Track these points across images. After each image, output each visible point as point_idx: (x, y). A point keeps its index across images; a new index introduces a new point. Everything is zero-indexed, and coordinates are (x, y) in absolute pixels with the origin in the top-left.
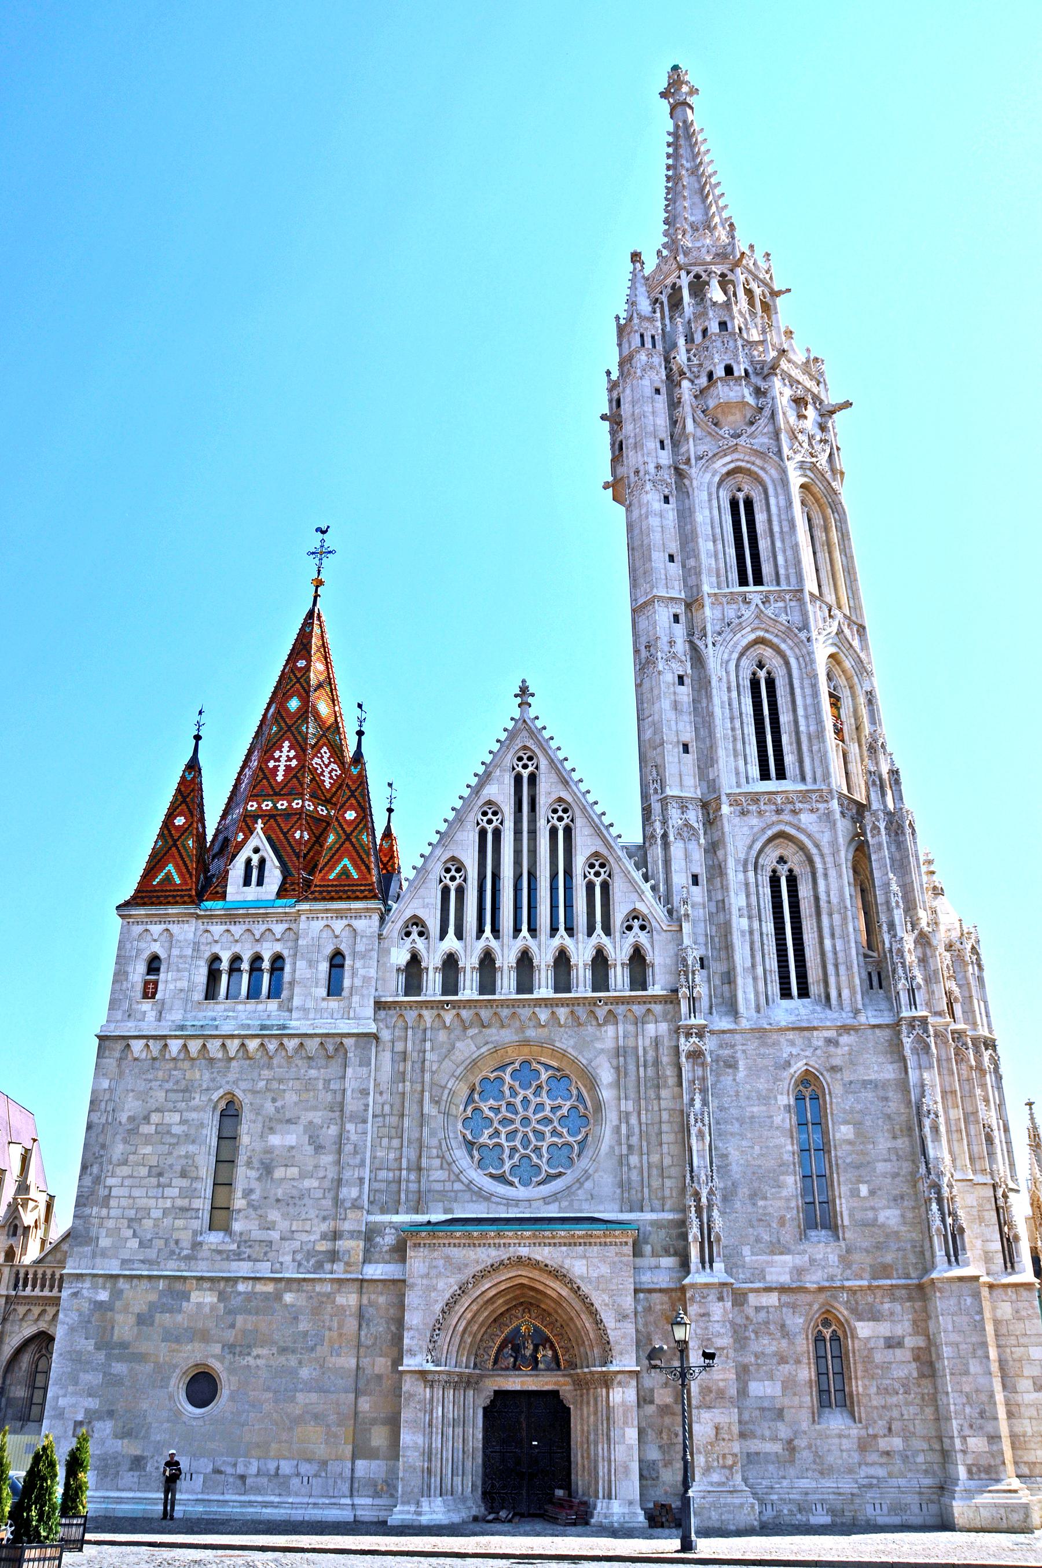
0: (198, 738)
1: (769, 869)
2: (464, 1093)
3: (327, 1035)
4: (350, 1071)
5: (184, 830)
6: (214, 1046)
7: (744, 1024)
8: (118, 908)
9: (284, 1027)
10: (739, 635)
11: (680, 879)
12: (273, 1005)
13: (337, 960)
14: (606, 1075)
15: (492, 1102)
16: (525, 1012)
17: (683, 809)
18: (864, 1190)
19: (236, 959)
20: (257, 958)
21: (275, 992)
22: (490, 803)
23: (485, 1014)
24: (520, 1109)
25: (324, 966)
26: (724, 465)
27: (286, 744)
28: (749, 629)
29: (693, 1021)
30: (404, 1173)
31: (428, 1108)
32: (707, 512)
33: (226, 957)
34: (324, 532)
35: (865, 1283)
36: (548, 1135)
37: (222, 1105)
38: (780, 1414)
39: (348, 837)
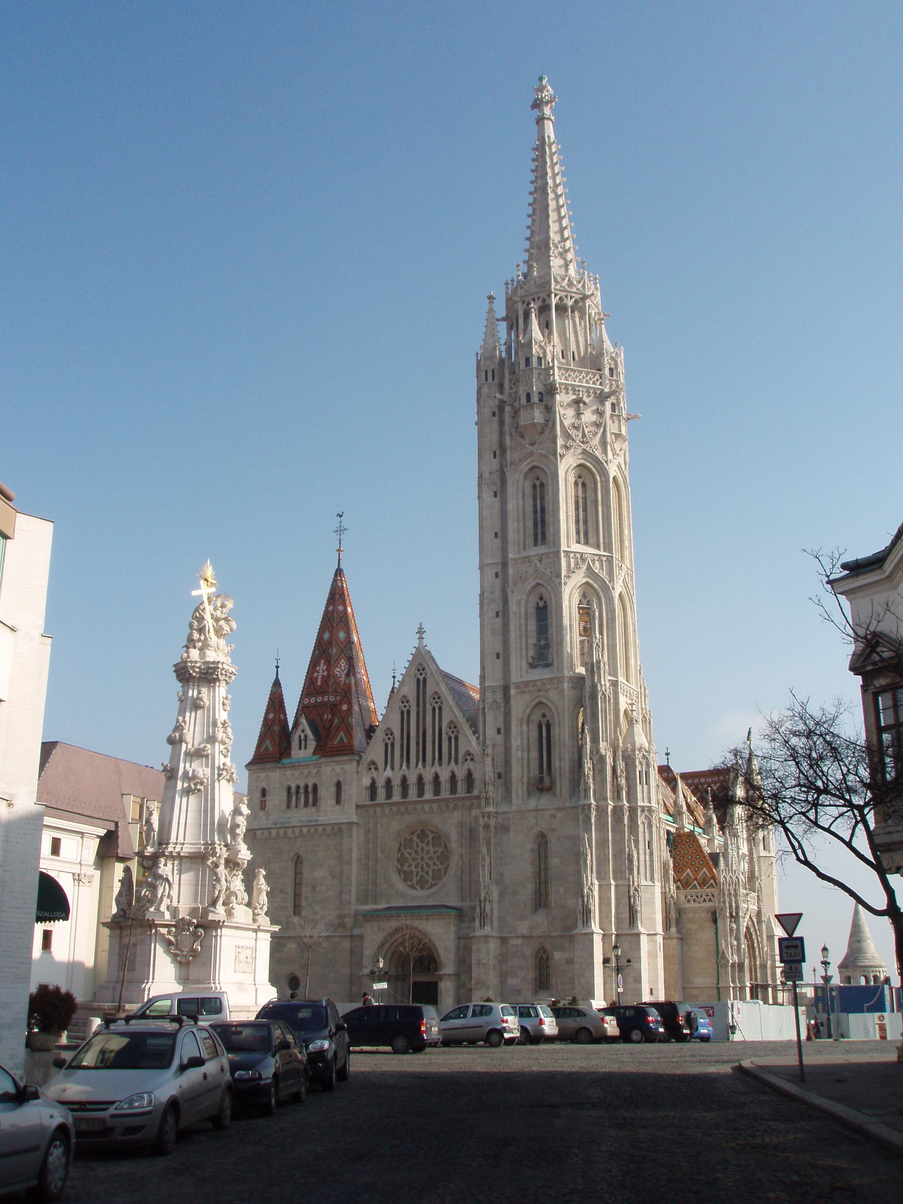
0: (277, 667)
1: (537, 722)
2: (396, 846)
3: (335, 824)
4: (344, 841)
5: (273, 721)
6: (289, 831)
7: (514, 808)
8: (246, 766)
9: (316, 821)
10: (526, 583)
11: (491, 732)
12: (314, 809)
13: (339, 785)
14: (454, 836)
15: (409, 850)
16: (419, 807)
17: (494, 692)
18: (562, 890)
19: (298, 787)
20: (307, 787)
21: (315, 804)
22: (404, 697)
23: (402, 808)
24: (420, 853)
25: (333, 789)
26: (527, 465)
27: (322, 662)
28: (532, 579)
29: (487, 809)
30: (370, 886)
31: (380, 855)
32: (515, 502)
33: (293, 787)
34: (341, 516)
35: (557, 934)
36: (432, 865)
37: (296, 858)
38: (519, 992)
39: (343, 721)
